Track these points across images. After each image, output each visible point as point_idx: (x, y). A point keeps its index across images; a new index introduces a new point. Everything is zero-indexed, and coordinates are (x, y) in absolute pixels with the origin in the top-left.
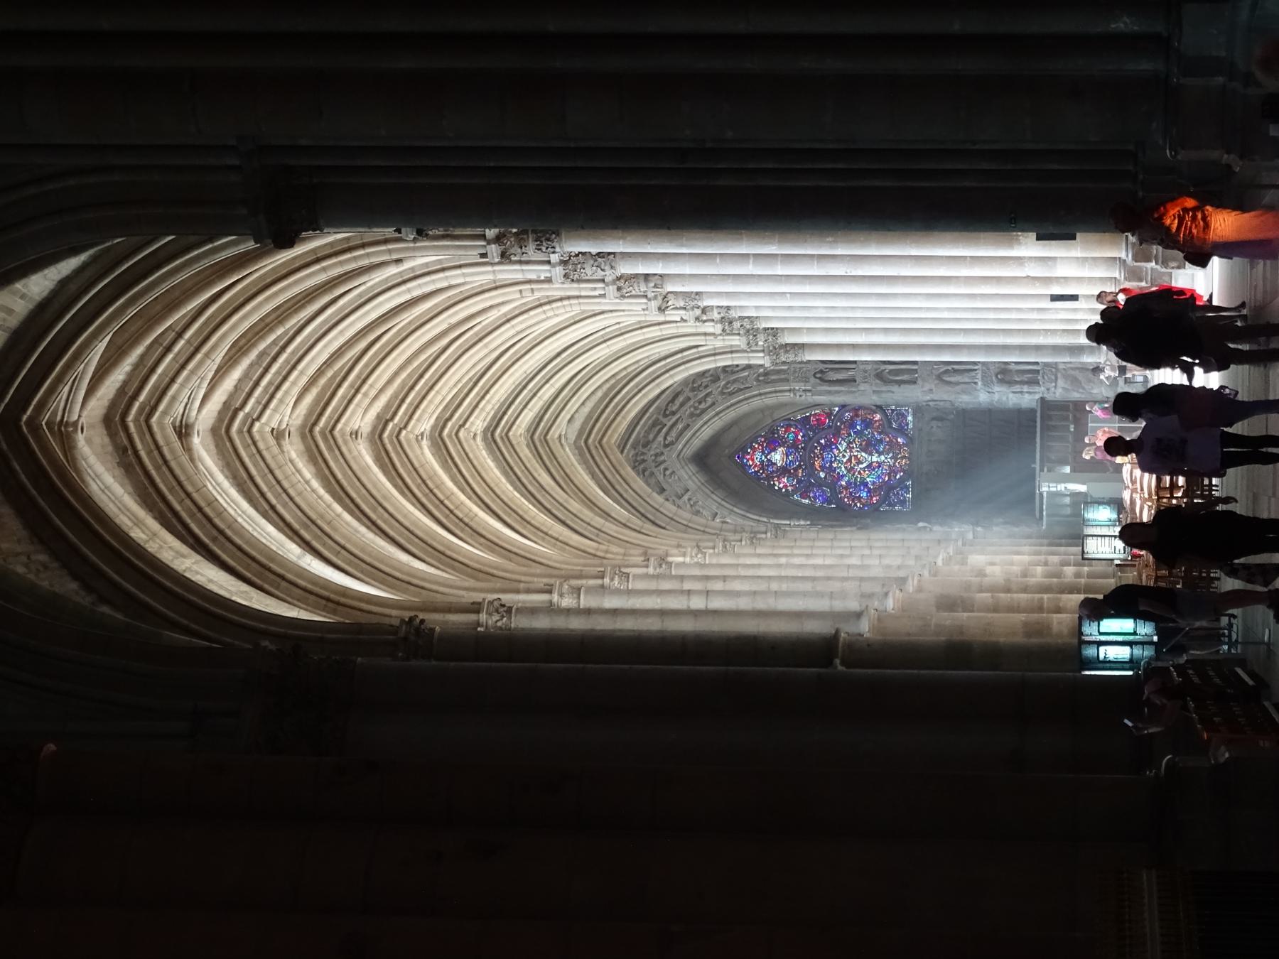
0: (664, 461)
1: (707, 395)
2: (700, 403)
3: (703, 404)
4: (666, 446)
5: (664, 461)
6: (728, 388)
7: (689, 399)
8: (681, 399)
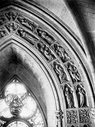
0: (9, 31)
1: (53, 56)
2: (47, 51)
3: (47, 53)
4: (19, 31)
5: (9, 31)
6: (58, 68)
7: (50, 44)
8: (49, 40)
